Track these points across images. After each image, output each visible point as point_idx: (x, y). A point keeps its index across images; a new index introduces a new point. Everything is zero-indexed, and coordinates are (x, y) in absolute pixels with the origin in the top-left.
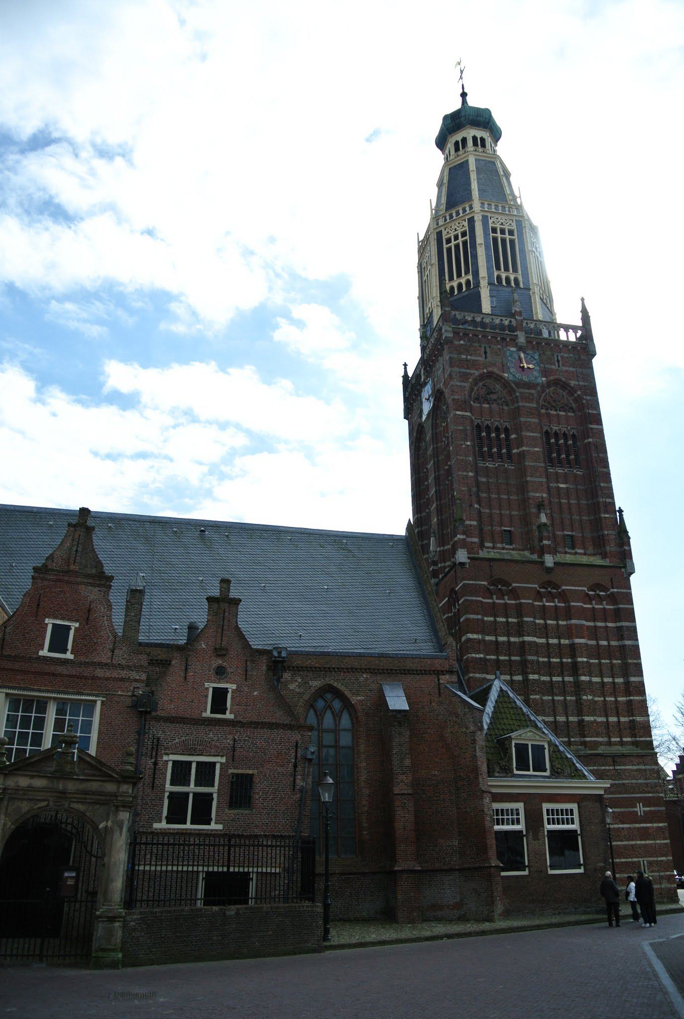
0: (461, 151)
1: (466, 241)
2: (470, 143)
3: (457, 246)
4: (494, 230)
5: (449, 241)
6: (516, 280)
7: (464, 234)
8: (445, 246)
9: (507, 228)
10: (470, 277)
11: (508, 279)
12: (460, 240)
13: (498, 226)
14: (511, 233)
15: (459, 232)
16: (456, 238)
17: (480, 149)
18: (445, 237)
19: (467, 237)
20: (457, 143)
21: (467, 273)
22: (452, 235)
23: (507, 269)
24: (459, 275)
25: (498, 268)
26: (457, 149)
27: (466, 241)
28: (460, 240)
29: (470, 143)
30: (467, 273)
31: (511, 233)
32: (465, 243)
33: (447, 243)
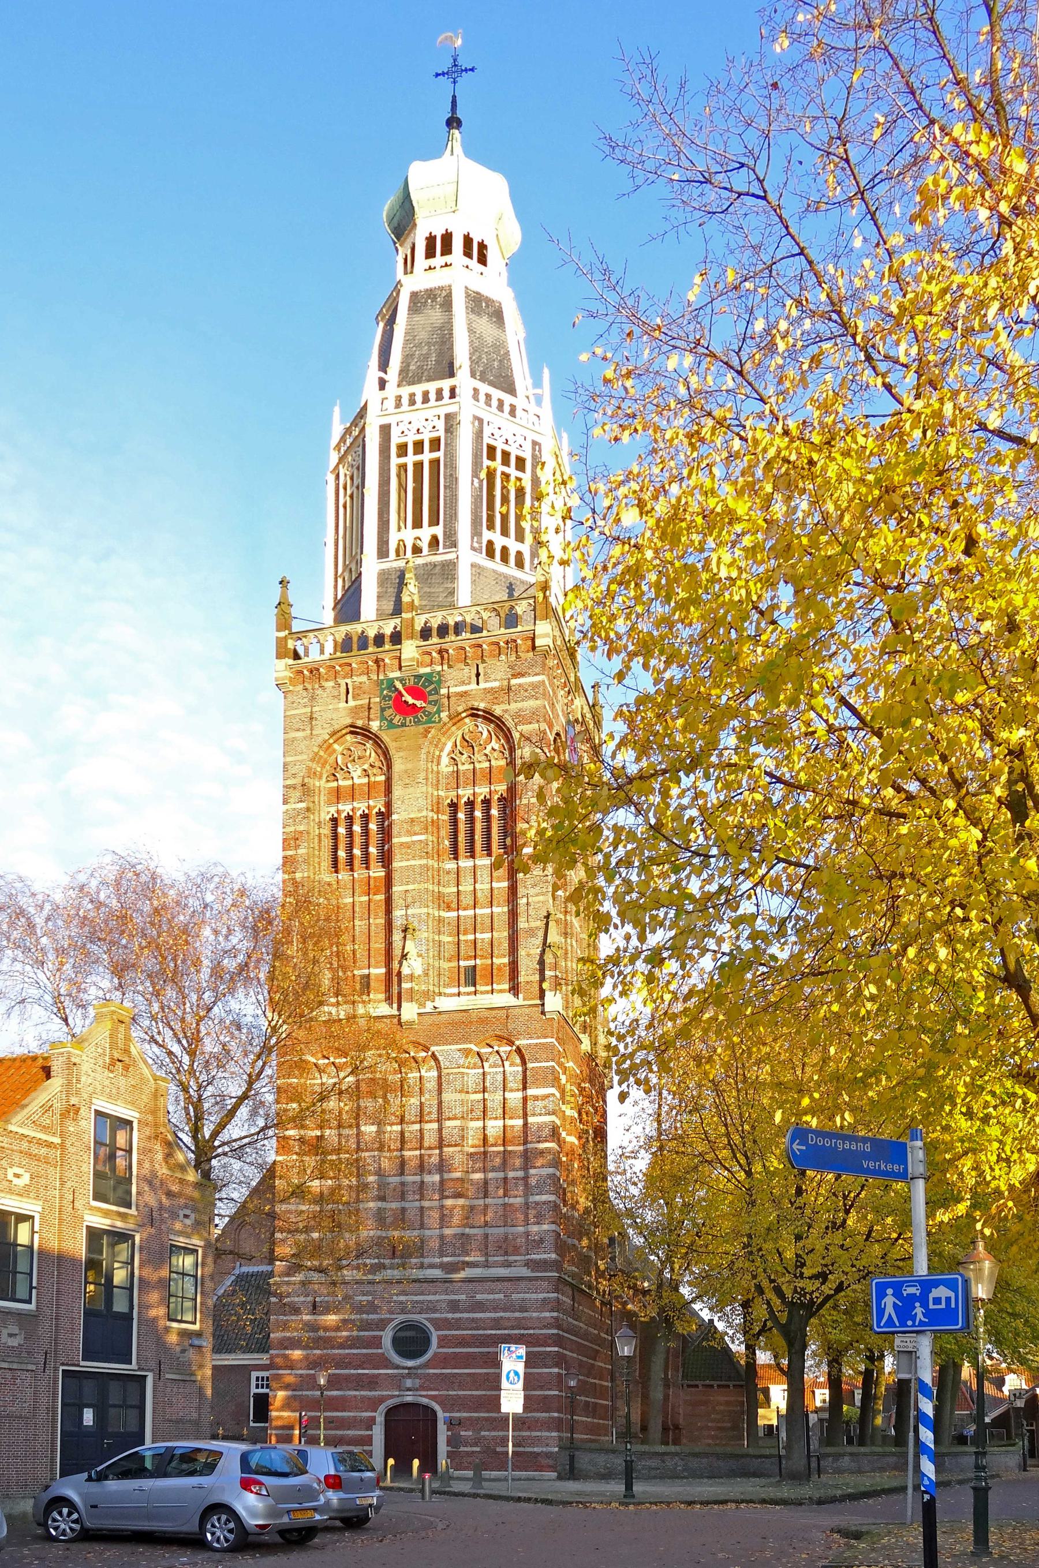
0: (439, 260)
1: (438, 461)
2: (458, 245)
3: (419, 466)
4: (491, 450)
5: (402, 450)
6: (519, 554)
7: (435, 444)
8: (395, 461)
9: (514, 452)
10: (439, 531)
11: (505, 550)
12: (427, 457)
13: (500, 446)
14: (521, 463)
15: (426, 437)
16: (419, 447)
17: (474, 263)
18: (395, 440)
19: (440, 454)
20: (431, 240)
21: (434, 521)
22: (410, 439)
23: (505, 532)
24: (417, 524)
25: (491, 527)
26: (430, 253)
27: (438, 461)
28: (427, 457)
29: (458, 245)
30: (434, 521)
31: (521, 463)
32: (435, 463)
33: (399, 456)
